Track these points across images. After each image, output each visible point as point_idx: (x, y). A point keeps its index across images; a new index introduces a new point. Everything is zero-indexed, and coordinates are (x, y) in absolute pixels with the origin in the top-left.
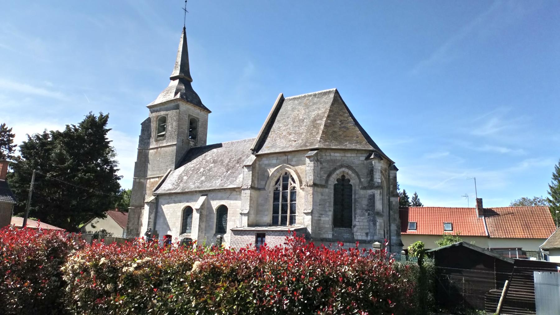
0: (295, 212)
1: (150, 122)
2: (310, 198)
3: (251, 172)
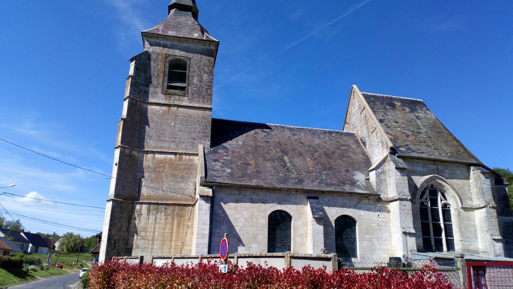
1: (149, 59)
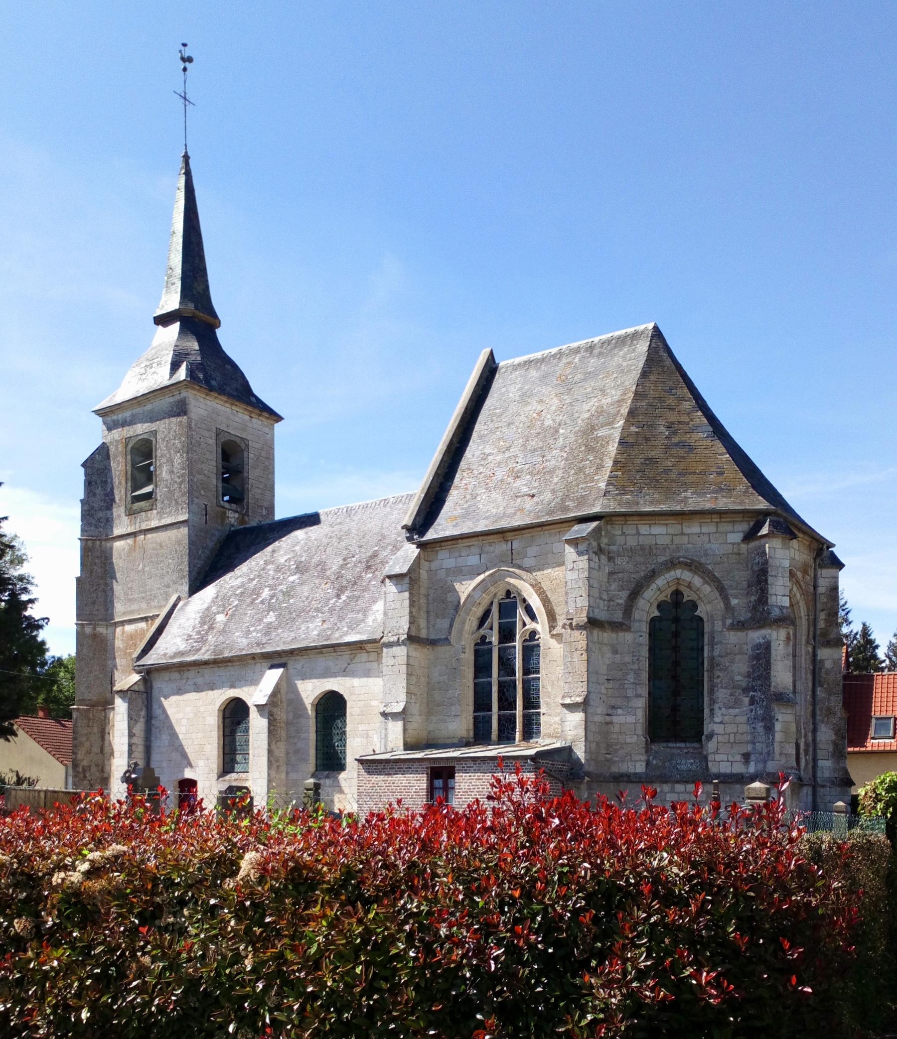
0: (539, 703)
2: (580, 664)
3: (407, 594)
